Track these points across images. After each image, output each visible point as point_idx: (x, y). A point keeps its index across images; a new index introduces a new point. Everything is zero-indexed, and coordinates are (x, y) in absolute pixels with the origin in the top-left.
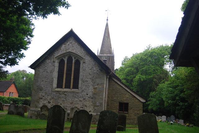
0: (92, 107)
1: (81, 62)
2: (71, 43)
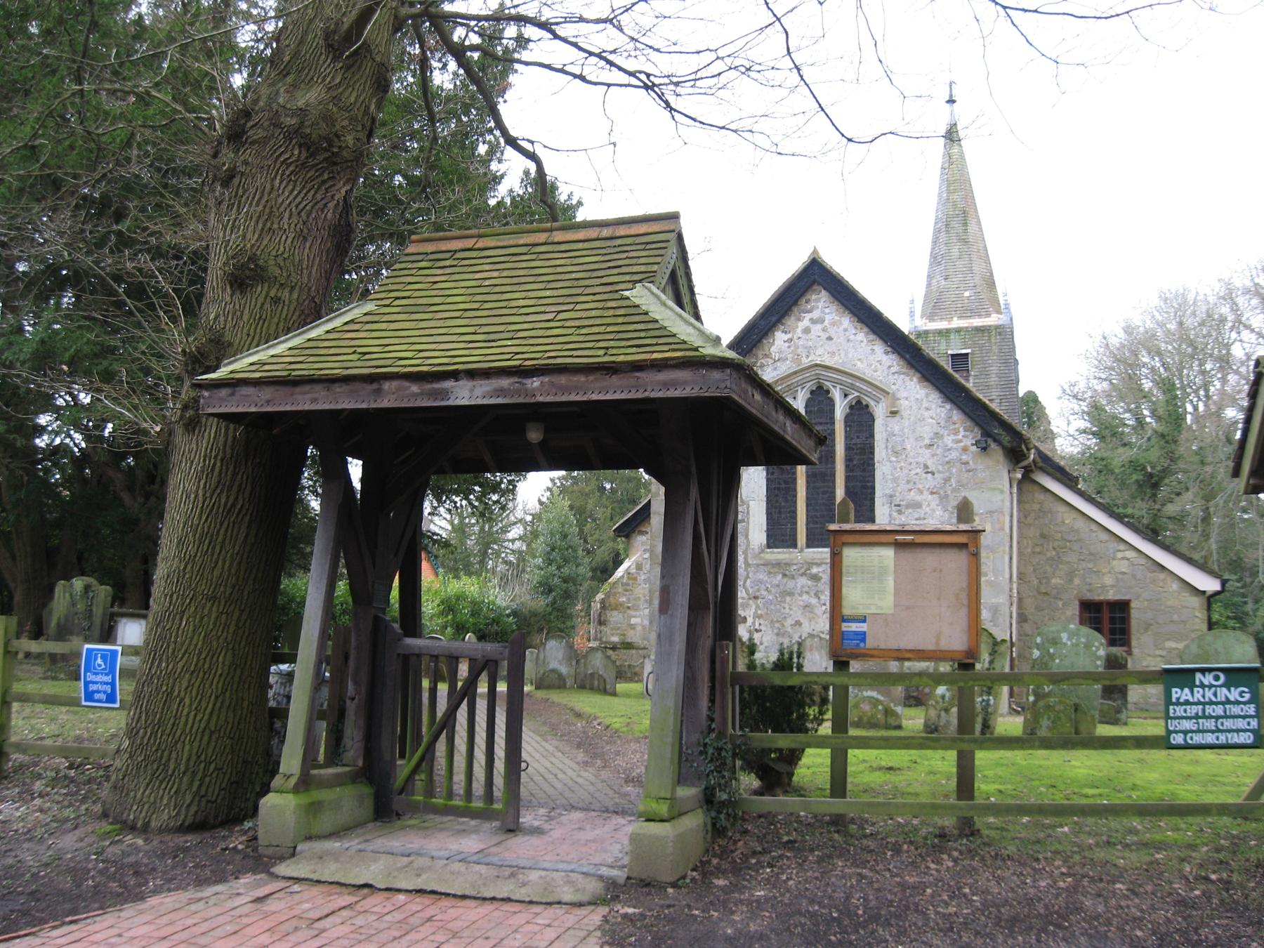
1: (879, 411)
2: (820, 321)
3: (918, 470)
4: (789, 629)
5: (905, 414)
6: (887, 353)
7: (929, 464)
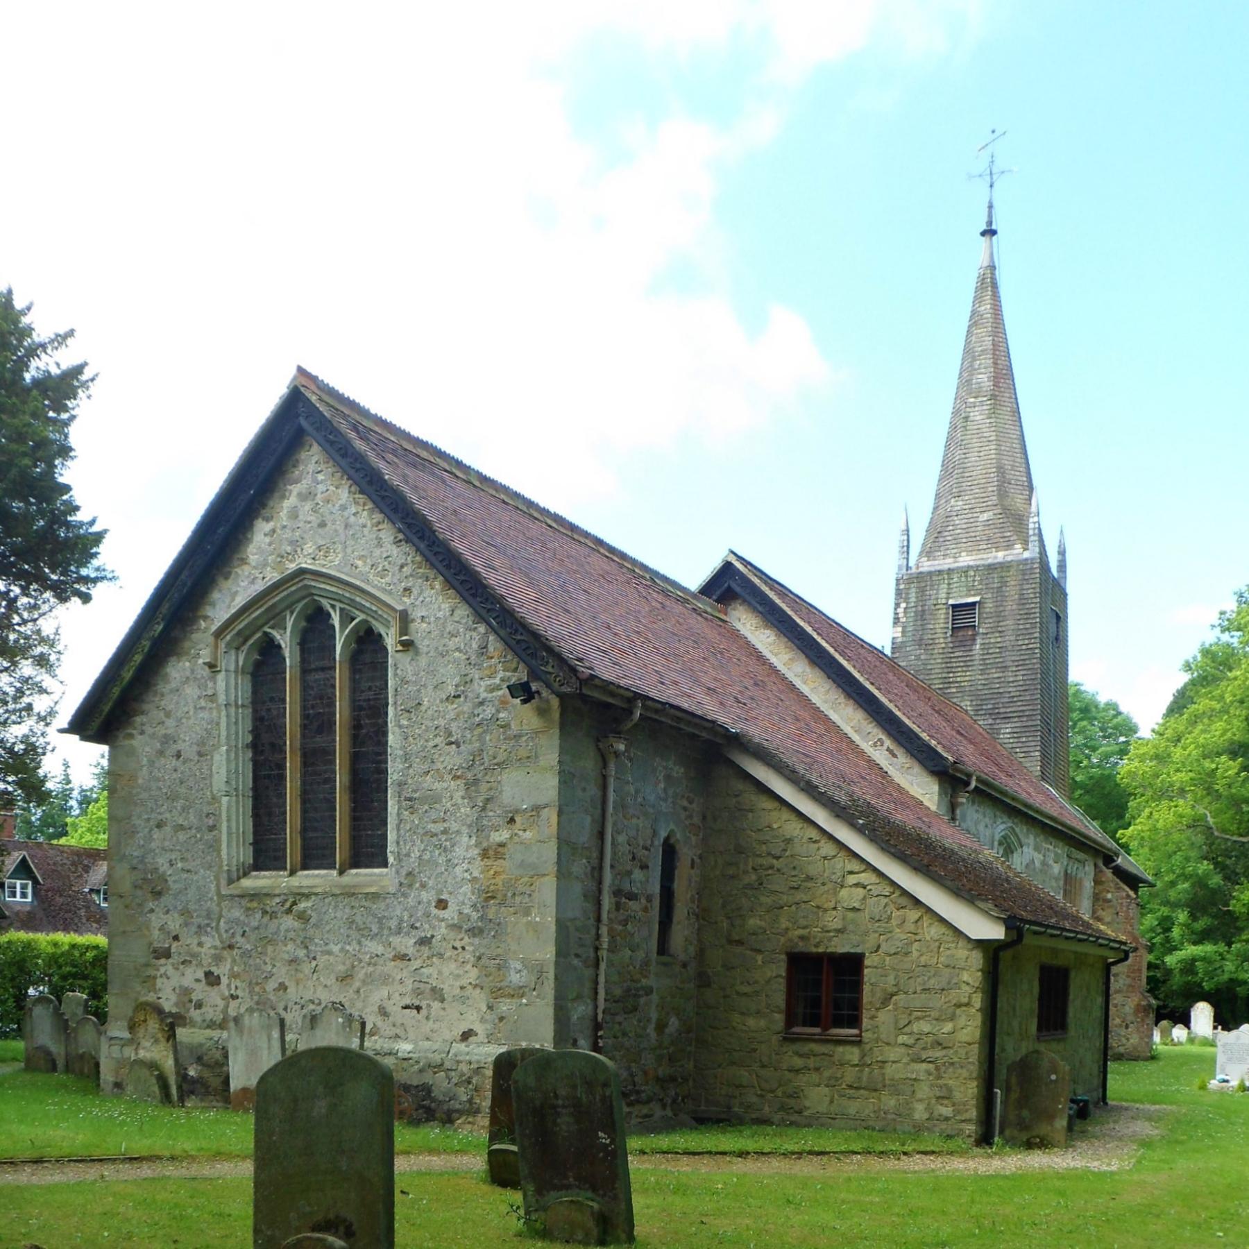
0: (480, 1000)
3: (438, 740)
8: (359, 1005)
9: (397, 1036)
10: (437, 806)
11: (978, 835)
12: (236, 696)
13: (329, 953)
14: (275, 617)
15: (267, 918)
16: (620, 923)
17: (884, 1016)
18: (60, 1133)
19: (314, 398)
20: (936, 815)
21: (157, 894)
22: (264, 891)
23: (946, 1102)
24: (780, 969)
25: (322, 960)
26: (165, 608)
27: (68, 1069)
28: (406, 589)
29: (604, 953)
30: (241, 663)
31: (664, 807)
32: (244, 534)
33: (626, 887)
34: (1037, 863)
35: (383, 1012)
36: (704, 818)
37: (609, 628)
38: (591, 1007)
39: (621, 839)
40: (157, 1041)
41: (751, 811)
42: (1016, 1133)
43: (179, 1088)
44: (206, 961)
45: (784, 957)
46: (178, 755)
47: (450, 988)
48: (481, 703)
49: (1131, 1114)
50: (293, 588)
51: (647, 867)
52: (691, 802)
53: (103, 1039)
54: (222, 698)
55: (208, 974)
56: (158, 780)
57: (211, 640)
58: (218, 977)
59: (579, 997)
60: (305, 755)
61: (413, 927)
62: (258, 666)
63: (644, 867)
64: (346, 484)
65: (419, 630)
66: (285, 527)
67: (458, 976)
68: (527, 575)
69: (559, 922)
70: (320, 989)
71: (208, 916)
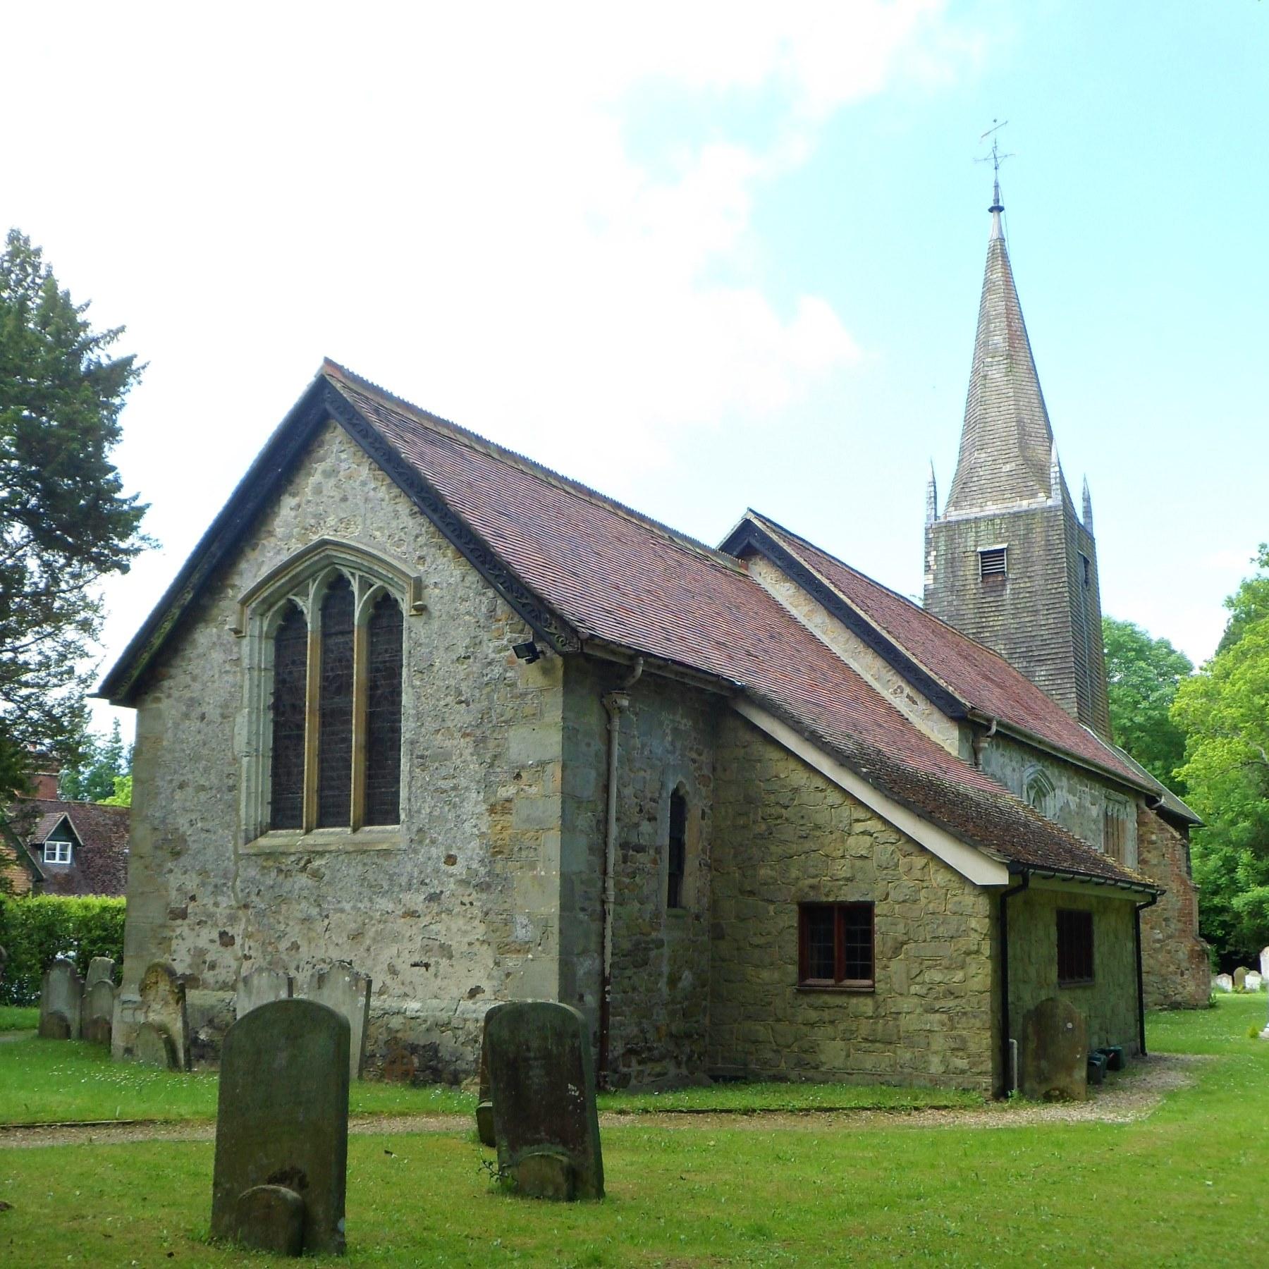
4: (284, 956)
5: (435, 609)
6: (413, 514)
7: (463, 687)
8: (369, 963)
9: (406, 995)
10: (448, 763)
11: (1004, 782)
12: (260, 661)
13: (342, 911)
14: (298, 585)
15: (282, 877)
16: (628, 875)
17: (895, 965)
18: (59, 1097)
19: (338, 386)
20: (957, 760)
21: (176, 855)
22: (281, 850)
23: (961, 1054)
24: (790, 919)
25: (335, 917)
26: (195, 578)
27: (81, 1035)
28: (420, 558)
29: (610, 907)
30: (265, 629)
31: (671, 759)
32: (272, 508)
33: (634, 839)
34: (1069, 809)
35: (393, 971)
36: (714, 769)
37: (618, 588)
38: (598, 962)
39: (628, 791)
40: (166, 1003)
41: (760, 761)
42: (1036, 1086)
43: (187, 1051)
44: (222, 920)
45: (795, 907)
46: (203, 717)
47: (458, 944)
48: (490, 664)
49: (1169, 1064)
50: (316, 558)
51: (655, 819)
52: (700, 755)
53: (116, 1002)
54: (246, 663)
55: (223, 934)
56: (182, 742)
57: (238, 606)
58: (233, 937)
59: (584, 952)
60: (323, 715)
61: (423, 883)
62: (282, 630)
63: (652, 819)
64: (366, 462)
65: (432, 595)
66: (309, 501)
67: (466, 932)
68: (537, 542)
69: (563, 875)
70: (331, 947)
71: (225, 876)
